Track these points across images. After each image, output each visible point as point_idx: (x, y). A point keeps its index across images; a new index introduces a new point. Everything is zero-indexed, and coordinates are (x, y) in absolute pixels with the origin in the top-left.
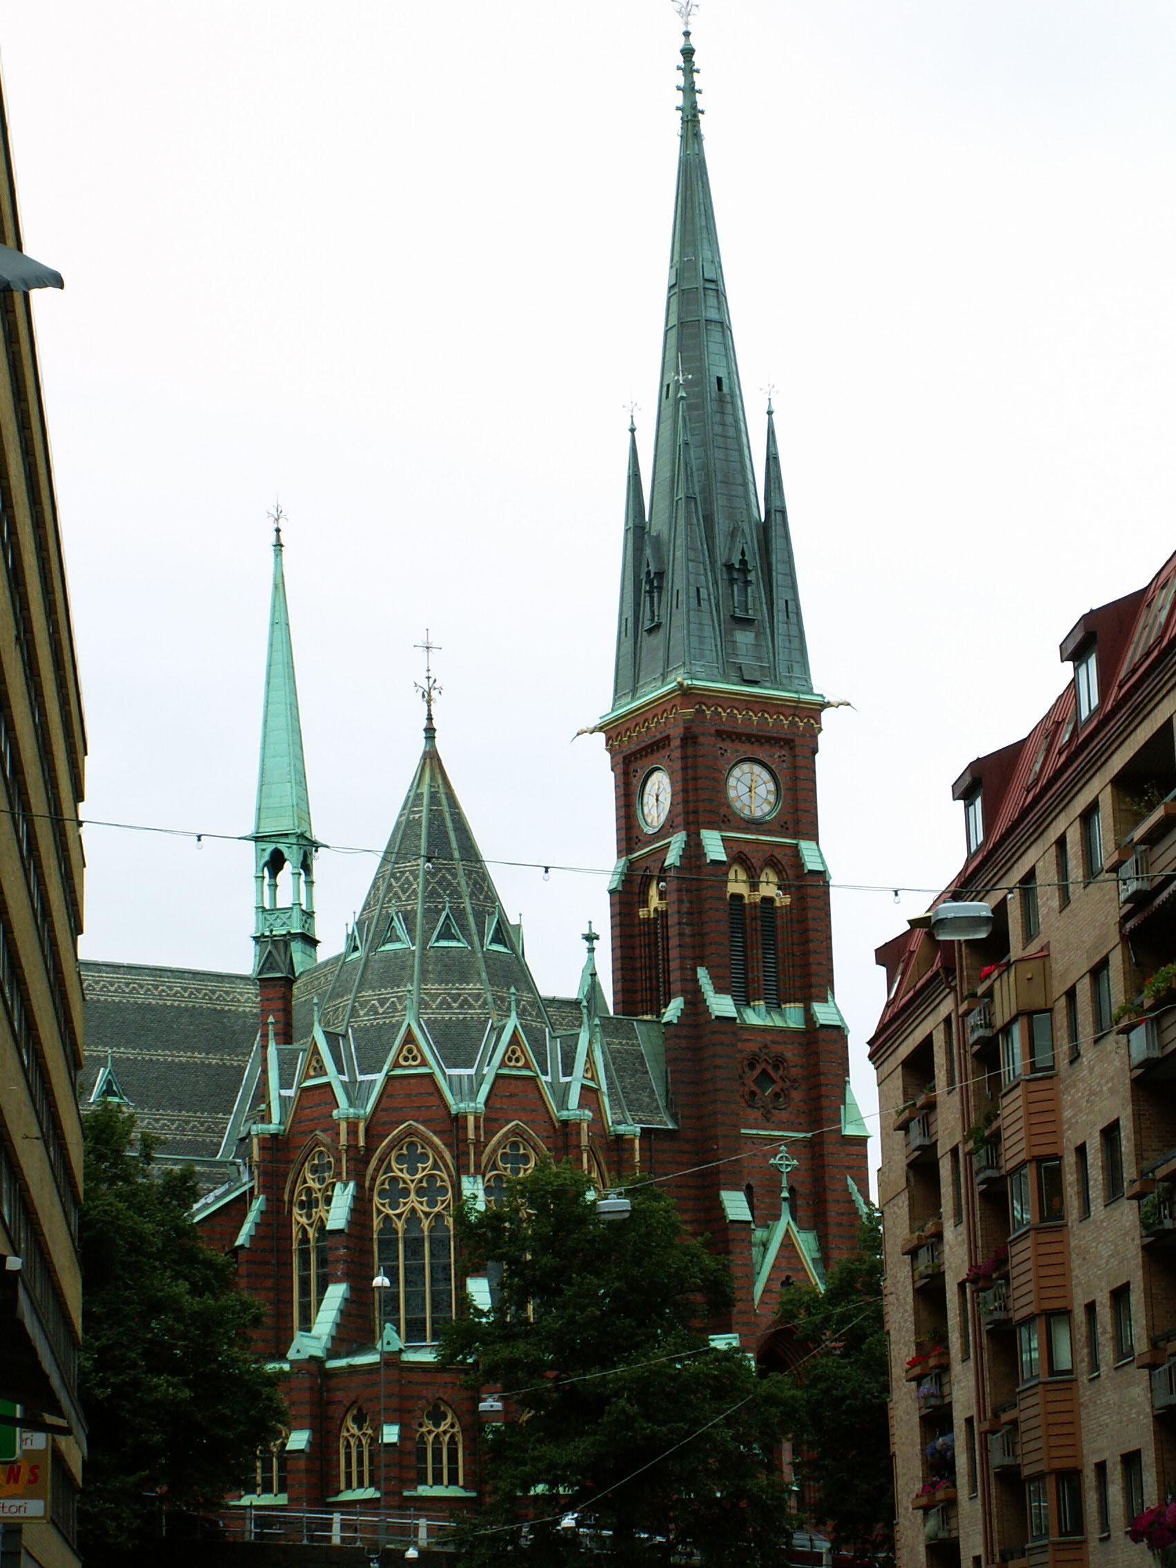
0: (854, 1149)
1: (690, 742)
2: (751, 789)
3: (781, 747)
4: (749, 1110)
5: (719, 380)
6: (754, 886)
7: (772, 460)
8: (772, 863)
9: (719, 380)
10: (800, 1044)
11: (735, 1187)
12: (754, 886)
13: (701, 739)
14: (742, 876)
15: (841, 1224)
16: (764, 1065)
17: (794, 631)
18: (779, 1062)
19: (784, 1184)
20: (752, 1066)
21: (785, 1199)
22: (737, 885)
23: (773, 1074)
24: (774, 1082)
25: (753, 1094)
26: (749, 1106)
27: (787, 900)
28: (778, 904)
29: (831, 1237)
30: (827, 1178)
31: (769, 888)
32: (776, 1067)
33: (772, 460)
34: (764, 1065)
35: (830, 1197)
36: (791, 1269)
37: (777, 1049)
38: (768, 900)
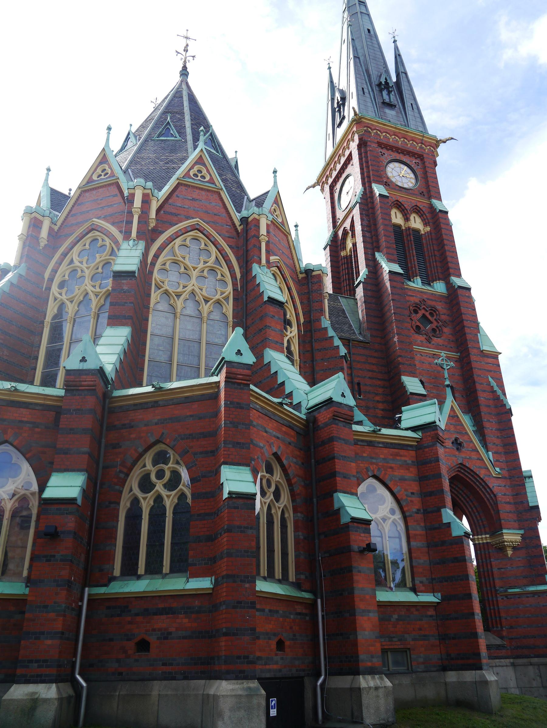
0: (490, 360)
1: (363, 146)
2: (401, 174)
3: (416, 158)
4: (416, 335)
5: (369, 30)
6: (407, 219)
7: (398, 57)
8: (417, 210)
9: (369, 30)
10: (446, 303)
11: (412, 374)
12: (407, 219)
13: (369, 143)
14: (399, 215)
15: (489, 406)
16: (423, 311)
17: (417, 115)
18: (433, 311)
19: (446, 375)
20: (416, 312)
21: (448, 386)
22: (397, 218)
23: (430, 317)
24: (431, 322)
25: (418, 327)
26: (417, 333)
27: (428, 229)
28: (423, 232)
29: (483, 414)
30: (475, 376)
31: (416, 223)
32: (431, 314)
33: (398, 57)
34: (423, 311)
35: (479, 387)
36: (457, 433)
37: (433, 303)
38: (417, 231)
